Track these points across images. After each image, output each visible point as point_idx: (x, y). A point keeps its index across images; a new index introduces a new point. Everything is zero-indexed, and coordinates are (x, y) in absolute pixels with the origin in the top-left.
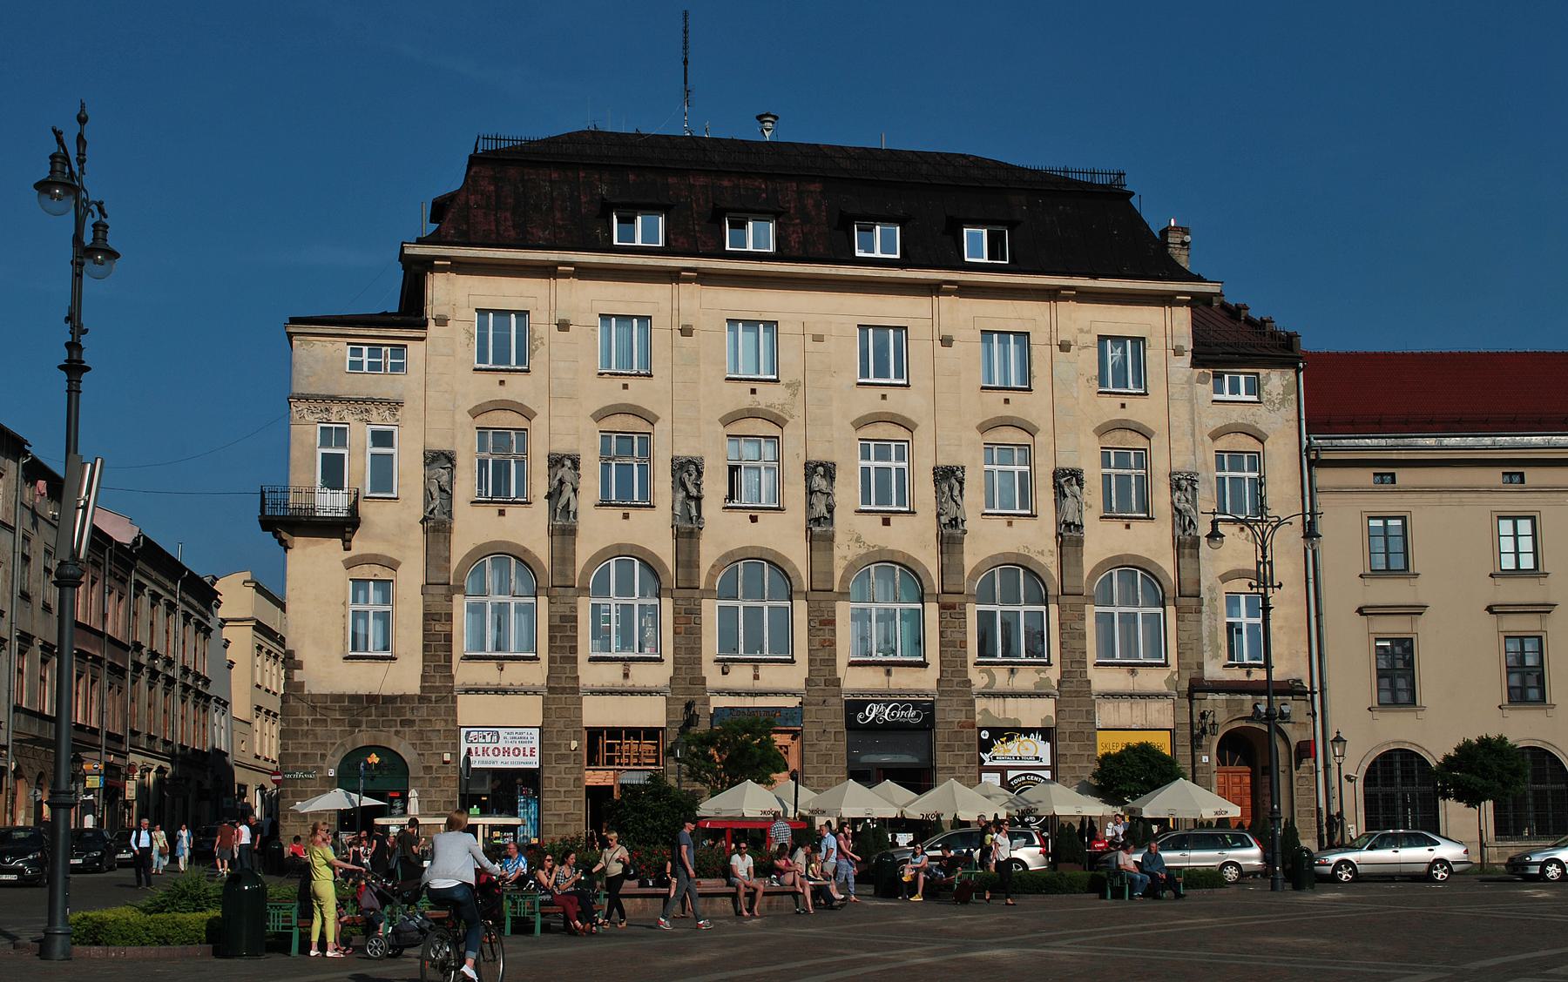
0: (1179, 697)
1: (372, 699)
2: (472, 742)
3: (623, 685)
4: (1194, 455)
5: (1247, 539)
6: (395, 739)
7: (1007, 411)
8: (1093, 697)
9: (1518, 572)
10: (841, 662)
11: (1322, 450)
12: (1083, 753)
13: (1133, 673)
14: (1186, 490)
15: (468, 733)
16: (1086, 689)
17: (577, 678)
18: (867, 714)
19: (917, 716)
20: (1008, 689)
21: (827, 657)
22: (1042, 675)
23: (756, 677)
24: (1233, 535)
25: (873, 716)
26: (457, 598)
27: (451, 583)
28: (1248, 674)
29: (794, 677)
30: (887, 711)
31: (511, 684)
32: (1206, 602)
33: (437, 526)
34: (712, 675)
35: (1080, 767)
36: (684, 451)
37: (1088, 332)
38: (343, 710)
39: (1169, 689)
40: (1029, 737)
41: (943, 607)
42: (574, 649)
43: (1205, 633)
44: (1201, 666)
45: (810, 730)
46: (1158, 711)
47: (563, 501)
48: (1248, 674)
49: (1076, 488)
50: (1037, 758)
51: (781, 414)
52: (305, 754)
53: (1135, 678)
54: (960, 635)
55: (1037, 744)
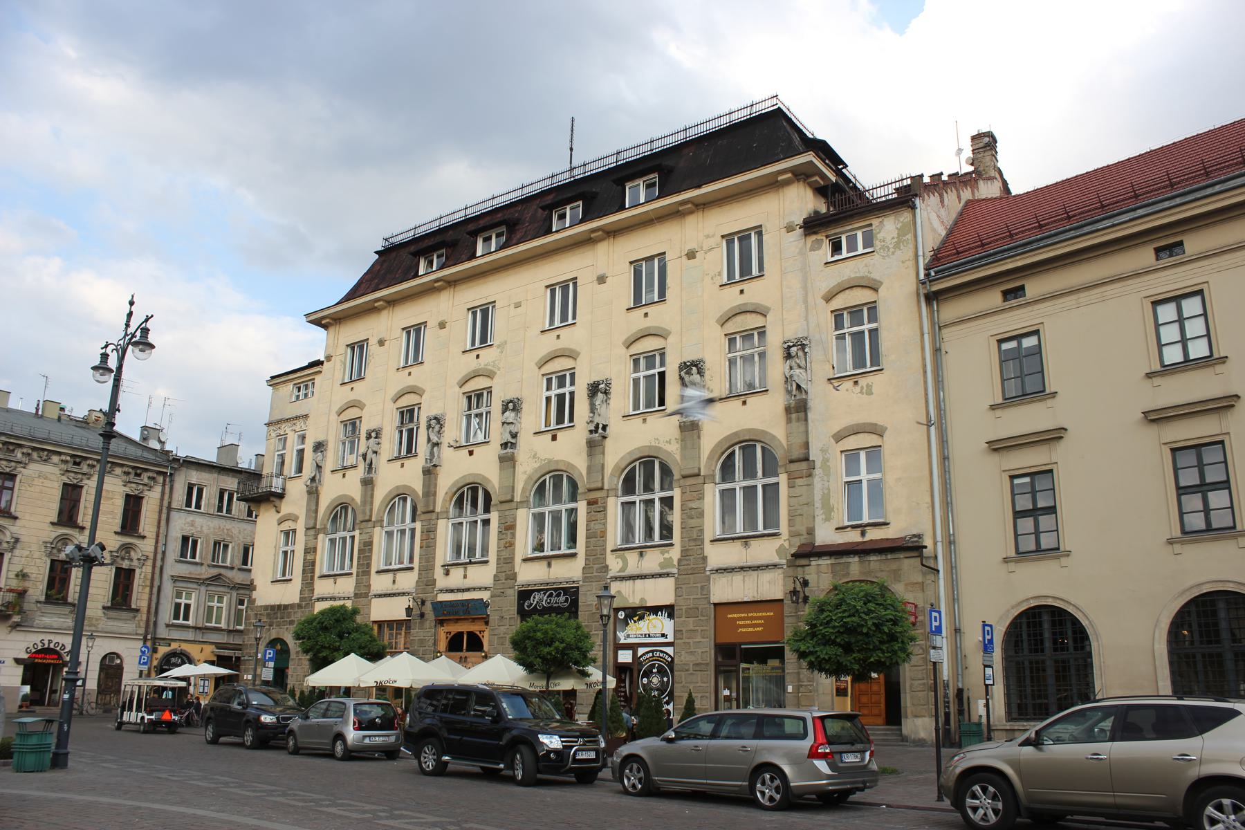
0: (788, 567)
1: (279, 606)
3: (392, 589)
4: (807, 319)
5: (861, 392)
6: (286, 633)
7: (647, 323)
8: (708, 573)
9: (1188, 364)
10: (518, 559)
12: (696, 628)
13: (746, 544)
16: (701, 566)
17: (369, 586)
18: (532, 602)
19: (566, 601)
20: (636, 572)
21: (508, 556)
22: (666, 556)
23: (465, 577)
24: (847, 390)
25: (535, 603)
26: (321, 536)
27: (318, 527)
28: (863, 534)
29: (483, 576)
30: (545, 598)
31: (339, 593)
32: (818, 464)
33: (313, 492)
34: (441, 581)
35: (694, 642)
36: (433, 413)
37: (713, 236)
38: (268, 615)
39: (780, 559)
40: (657, 615)
41: (589, 504)
42: (369, 565)
43: (818, 496)
44: (811, 532)
45: (494, 618)
46: (769, 582)
47: (368, 461)
48: (863, 534)
49: (696, 377)
50: (663, 635)
51: (492, 368)
52: (251, 644)
53: (748, 550)
54: (601, 526)
55: (664, 621)
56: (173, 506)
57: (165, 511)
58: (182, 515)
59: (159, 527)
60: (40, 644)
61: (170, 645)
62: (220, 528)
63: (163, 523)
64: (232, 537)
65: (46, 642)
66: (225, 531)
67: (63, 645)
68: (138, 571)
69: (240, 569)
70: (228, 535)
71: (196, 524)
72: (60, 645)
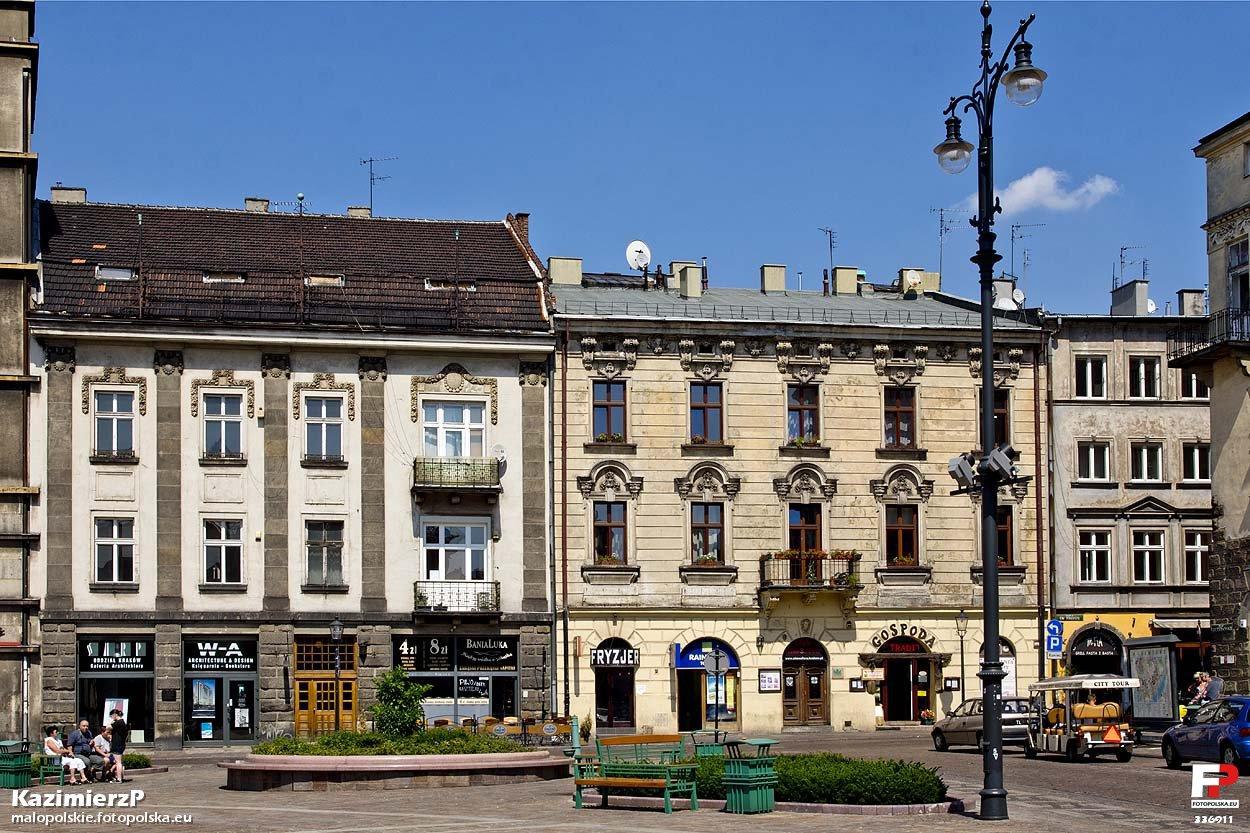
56: (1056, 397)
57: (1043, 407)
58: (1074, 409)
59: (1037, 433)
60: (890, 632)
61: (1081, 619)
62: (1138, 422)
63: (1043, 427)
64: (1161, 432)
65: (899, 629)
66: (1148, 425)
67: (923, 630)
68: (1015, 508)
69: (1181, 486)
70: (1153, 431)
71: (1099, 421)
72: (919, 631)
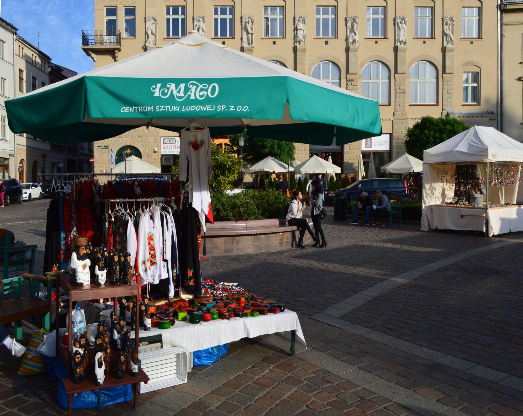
2: (165, 143)
11: (508, 4)
14: (449, 25)
15: (164, 140)
